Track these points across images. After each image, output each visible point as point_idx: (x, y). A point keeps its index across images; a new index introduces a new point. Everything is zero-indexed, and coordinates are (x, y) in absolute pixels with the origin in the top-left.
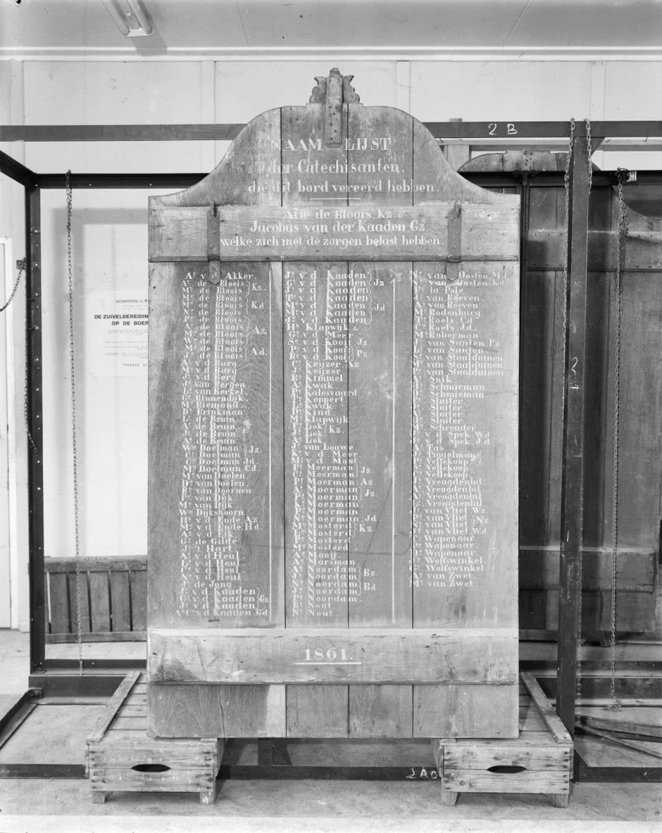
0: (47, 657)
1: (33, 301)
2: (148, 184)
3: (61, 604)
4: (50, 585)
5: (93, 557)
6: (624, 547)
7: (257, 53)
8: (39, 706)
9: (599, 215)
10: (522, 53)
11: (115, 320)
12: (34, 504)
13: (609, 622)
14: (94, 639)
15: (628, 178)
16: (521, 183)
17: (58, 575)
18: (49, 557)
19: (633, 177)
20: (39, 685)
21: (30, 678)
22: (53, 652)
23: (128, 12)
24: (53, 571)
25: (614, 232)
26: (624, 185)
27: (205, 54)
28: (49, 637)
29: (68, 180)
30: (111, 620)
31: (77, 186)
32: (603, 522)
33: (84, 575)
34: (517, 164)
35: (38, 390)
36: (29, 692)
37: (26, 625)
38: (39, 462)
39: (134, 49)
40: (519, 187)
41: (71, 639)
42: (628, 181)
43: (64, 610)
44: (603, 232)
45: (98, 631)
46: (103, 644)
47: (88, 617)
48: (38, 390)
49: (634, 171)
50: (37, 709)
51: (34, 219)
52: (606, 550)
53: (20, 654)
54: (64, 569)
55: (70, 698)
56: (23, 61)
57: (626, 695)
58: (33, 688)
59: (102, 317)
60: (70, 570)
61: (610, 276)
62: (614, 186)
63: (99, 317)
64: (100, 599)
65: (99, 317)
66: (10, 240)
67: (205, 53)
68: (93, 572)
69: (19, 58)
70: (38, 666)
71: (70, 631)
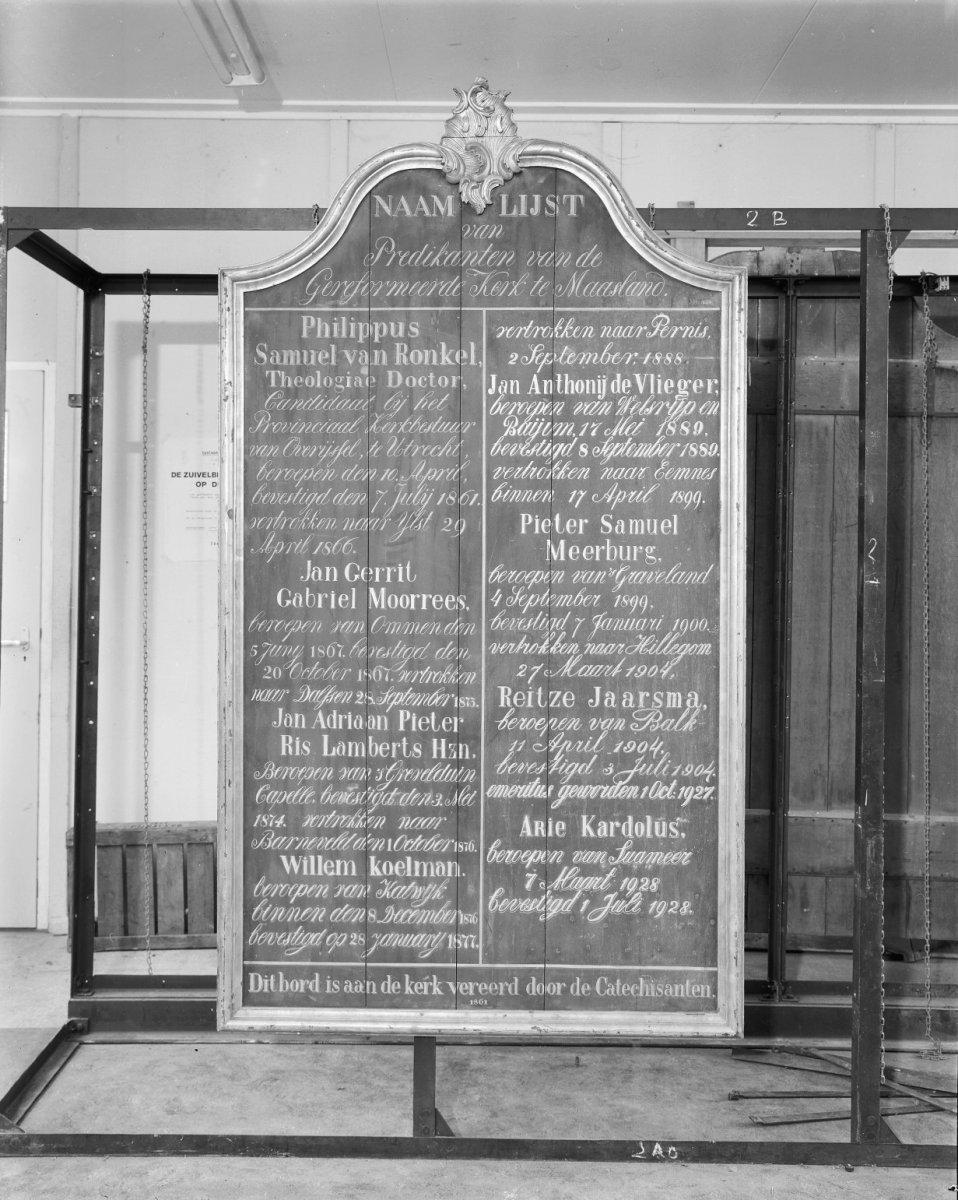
1: (91, 451)
3: (113, 893)
6: (940, 815)
7: (408, 110)
9: (901, 340)
10: (778, 112)
11: (202, 480)
12: (84, 745)
13: (920, 924)
14: (162, 946)
15: (937, 285)
19: (944, 285)
20: (83, 1014)
21: (70, 1003)
22: (105, 964)
23: (232, 52)
25: (917, 361)
26: (930, 295)
27: (334, 111)
30: (186, 916)
31: (158, 292)
32: (909, 778)
34: (779, 266)
35: (93, 579)
36: (69, 1024)
38: (92, 683)
39: (236, 102)
40: (782, 296)
41: (129, 944)
42: (937, 290)
43: (118, 901)
44: (901, 360)
45: (168, 932)
48: (93, 579)
49: (946, 276)
50: (79, 1051)
51: (94, 338)
52: (913, 818)
53: (53, 968)
54: (119, 842)
56: (80, 117)
57: (949, 1036)
59: (183, 475)
60: (130, 841)
61: (912, 423)
62: (916, 298)
63: (177, 475)
64: (171, 884)
65: (177, 475)
66: (53, 365)
69: (74, 113)
70: (83, 985)
71: (126, 933)
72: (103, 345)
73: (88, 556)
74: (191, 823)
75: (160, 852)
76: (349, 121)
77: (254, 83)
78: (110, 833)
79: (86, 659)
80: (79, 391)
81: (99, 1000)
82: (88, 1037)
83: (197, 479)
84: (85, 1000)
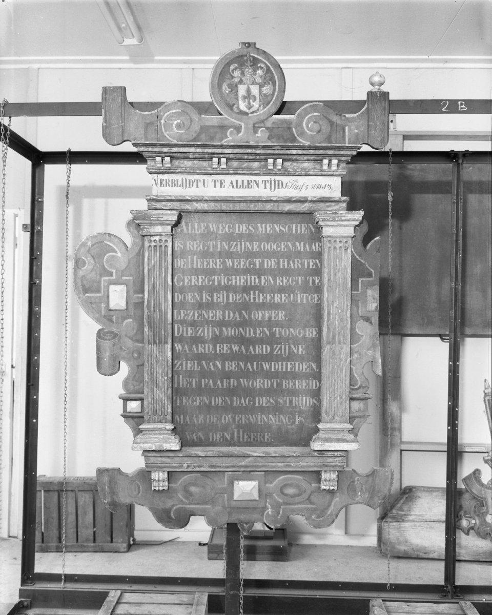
0: (36, 571)
1: (36, 258)
2: (136, 161)
4: (44, 500)
5: (81, 477)
12: (30, 435)
16: (457, 161)
17: (51, 493)
18: (45, 476)
20: (28, 597)
22: (44, 563)
24: (46, 489)
27: (185, 63)
29: (68, 157)
30: (94, 532)
31: (75, 162)
33: (74, 493)
36: (19, 603)
39: (127, 58)
41: (58, 550)
47: (75, 530)
48: (36, 334)
54: (56, 488)
56: (39, 69)
60: (60, 489)
67: (185, 62)
68: (81, 491)
69: (36, 66)
70: (28, 578)
72: (43, 195)
73: (33, 321)
75: (79, 494)
76: (193, 69)
77: (137, 43)
78: (51, 483)
79: (32, 383)
80: (28, 222)
82: (30, 611)
84: (29, 588)
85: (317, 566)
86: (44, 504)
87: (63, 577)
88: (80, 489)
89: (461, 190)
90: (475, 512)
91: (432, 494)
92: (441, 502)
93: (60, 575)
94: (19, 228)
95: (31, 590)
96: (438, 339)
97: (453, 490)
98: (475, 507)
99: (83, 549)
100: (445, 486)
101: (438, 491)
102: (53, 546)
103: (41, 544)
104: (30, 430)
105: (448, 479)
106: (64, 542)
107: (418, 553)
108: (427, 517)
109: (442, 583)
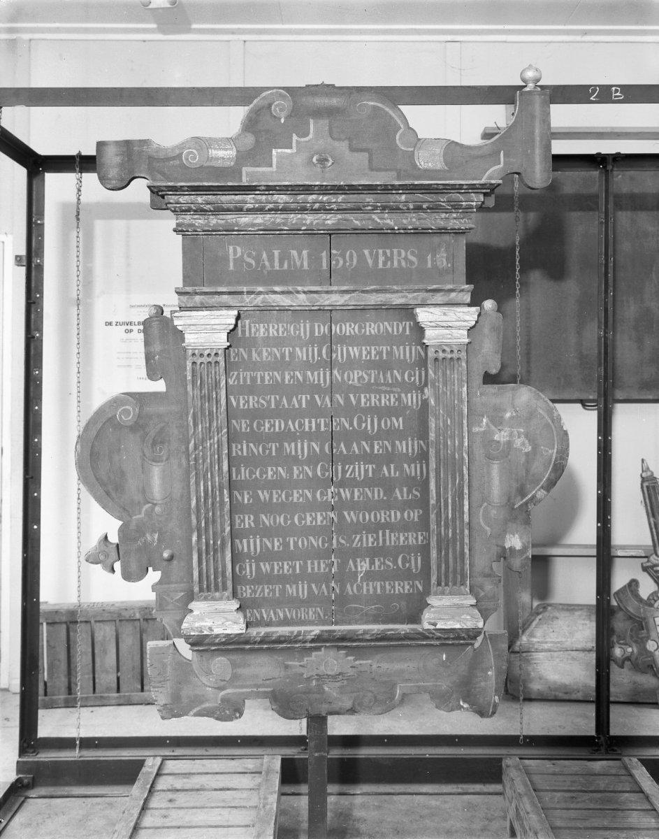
1: (34, 303)
3: (59, 661)
4: (47, 636)
5: (98, 603)
8: (28, 800)
11: (129, 327)
12: (29, 545)
14: (97, 703)
17: (56, 626)
18: (46, 602)
21: (18, 762)
22: (51, 724)
24: (50, 621)
28: (43, 700)
29: (77, 163)
30: (118, 679)
33: (88, 625)
35: (37, 408)
36: (17, 780)
37: (16, 684)
39: (154, 26)
41: (70, 703)
43: (63, 666)
46: (108, 708)
47: (91, 676)
48: (37, 408)
50: (25, 804)
51: (36, 210)
54: (64, 619)
55: (67, 788)
58: (20, 776)
59: (114, 324)
60: (70, 620)
63: (110, 324)
64: (106, 653)
65: (110, 324)
68: (99, 621)
70: (29, 746)
71: (70, 693)
72: (43, 215)
73: (32, 389)
74: (122, 602)
75: (97, 627)
76: (245, 41)
78: (56, 612)
79: (30, 473)
80: (23, 252)
81: (41, 759)
83: (126, 327)
84: (31, 760)
85: (423, 714)
86: (48, 641)
87: (78, 742)
88: (98, 619)
89: (611, 206)
90: (632, 637)
91: (574, 614)
92: (586, 624)
93: (74, 740)
94: (10, 261)
95: (32, 762)
96: (579, 405)
97: (605, 606)
98: (631, 630)
99: (102, 702)
100: (594, 602)
101: (581, 609)
102: (60, 699)
103: (44, 697)
104: (29, 541)
105: (598, 593)
106: (79, 693)
107: (557, 693)
108: (568, 644)
109: (593, 733)
